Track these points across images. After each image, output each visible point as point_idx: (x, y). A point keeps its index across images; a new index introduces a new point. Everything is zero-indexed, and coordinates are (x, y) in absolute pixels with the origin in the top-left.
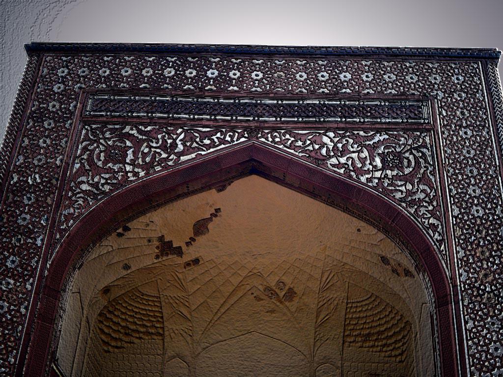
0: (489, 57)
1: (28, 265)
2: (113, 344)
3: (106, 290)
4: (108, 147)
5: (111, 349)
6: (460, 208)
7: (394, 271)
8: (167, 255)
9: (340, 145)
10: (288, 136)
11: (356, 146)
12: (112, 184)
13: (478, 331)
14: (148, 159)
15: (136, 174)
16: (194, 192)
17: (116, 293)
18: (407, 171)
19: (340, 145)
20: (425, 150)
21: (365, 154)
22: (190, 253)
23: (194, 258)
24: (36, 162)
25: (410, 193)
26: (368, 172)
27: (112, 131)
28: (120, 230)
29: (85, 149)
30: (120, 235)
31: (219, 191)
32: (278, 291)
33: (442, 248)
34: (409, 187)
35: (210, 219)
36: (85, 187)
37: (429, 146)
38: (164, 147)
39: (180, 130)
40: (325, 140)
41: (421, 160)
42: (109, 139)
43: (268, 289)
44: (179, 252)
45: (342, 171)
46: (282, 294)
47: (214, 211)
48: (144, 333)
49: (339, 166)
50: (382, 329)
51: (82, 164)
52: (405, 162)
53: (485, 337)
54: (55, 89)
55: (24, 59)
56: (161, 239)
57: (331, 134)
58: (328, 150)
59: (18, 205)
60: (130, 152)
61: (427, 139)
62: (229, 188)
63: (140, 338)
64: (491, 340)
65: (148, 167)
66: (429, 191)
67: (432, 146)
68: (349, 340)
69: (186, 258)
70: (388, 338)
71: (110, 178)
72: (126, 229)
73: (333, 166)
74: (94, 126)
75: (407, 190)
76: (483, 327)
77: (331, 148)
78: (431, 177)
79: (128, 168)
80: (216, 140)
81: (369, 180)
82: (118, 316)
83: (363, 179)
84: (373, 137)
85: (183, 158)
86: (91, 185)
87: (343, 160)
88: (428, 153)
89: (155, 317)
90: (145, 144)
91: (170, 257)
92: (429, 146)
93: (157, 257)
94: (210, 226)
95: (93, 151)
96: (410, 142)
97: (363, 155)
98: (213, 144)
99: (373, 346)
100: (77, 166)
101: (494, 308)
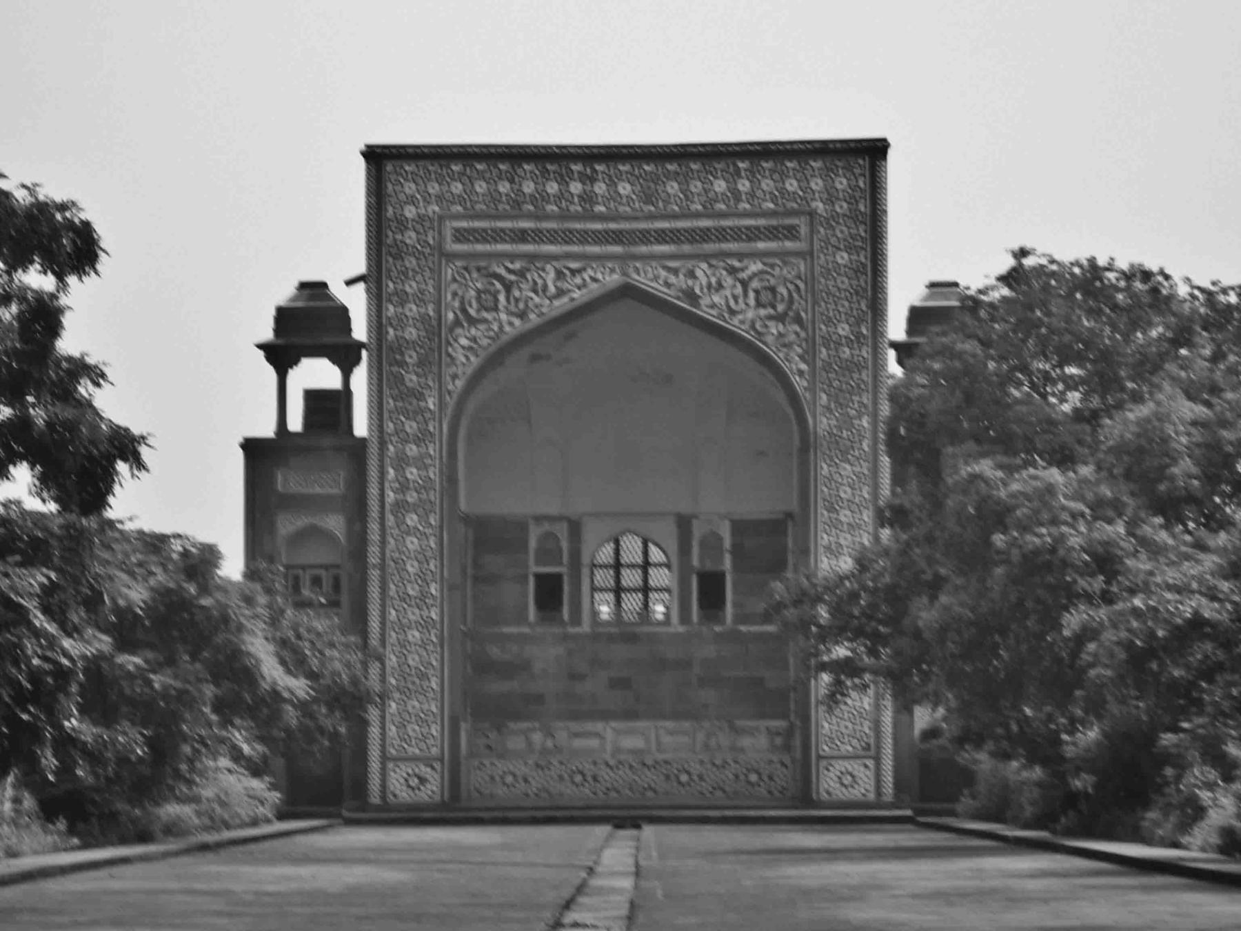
0: (876, 150)
4: (479, 292)
9: (713, 280)
12: (489, 338)
14: (521, 306)
15: (511, 324)
18: (781, 308)
19: (713, 280)
20: (798, 282)
27: (479, 269)
29: (455, 294)
34: (781, 327)
36: (464, 342)
38: (535, 291)
39: (548, 267)
44: (548, 357)
52: (779, 296)
54: (408, 215)
55: (361, 162)
58: (701, 289)
59: (402, 364)
60: (502, 298)
65: (522, 315)
66: (798, 329)
81: (742, 322)
83: (736, 321)
87: (716, 299)
88: (802, 286)
95: (463, 298)
100: (451, 316)
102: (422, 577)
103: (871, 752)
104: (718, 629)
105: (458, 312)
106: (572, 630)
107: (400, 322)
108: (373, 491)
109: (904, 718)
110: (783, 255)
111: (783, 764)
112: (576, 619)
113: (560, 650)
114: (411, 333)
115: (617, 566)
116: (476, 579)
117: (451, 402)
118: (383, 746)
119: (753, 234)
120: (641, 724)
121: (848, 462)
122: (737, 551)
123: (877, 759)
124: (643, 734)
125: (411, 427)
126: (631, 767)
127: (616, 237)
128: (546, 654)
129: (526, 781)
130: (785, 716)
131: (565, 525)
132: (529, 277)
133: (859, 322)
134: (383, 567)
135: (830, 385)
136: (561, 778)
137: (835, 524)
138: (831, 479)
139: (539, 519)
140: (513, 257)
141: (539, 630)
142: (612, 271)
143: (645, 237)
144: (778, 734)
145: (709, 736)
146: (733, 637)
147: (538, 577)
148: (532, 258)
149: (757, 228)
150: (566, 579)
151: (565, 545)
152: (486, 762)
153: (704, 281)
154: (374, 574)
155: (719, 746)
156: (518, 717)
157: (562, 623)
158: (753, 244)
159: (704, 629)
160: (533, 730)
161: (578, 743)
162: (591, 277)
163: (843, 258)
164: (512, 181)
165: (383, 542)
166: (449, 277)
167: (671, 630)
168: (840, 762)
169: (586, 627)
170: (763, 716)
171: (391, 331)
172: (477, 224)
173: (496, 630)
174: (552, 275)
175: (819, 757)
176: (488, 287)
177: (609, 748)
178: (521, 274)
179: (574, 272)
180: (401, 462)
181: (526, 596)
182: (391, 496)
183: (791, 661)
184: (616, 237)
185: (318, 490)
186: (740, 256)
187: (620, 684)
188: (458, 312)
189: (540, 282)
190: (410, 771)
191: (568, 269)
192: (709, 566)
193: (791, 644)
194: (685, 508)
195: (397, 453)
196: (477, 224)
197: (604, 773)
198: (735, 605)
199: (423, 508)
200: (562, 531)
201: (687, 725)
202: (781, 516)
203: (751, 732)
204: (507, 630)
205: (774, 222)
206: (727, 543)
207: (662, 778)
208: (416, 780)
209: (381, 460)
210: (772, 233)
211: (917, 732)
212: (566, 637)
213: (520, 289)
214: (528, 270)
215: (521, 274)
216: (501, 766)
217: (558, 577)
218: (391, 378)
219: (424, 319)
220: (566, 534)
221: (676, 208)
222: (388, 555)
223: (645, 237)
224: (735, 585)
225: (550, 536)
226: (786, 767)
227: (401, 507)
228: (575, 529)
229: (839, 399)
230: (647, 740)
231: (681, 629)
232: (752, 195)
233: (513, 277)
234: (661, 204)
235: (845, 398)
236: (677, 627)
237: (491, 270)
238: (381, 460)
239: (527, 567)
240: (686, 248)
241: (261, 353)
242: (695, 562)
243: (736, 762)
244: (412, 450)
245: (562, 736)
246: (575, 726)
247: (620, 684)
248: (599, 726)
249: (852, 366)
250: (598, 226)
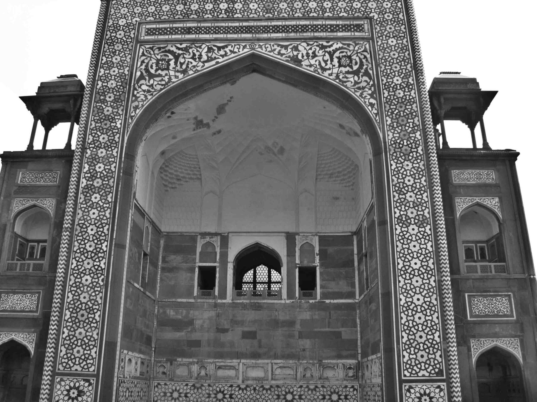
1: (113, 140)
2: (170, 186)
3: (163, 153)
4: (158, 61)
5: (168, 189)
6: (389, 92)
7: (348, 133)
8: (200, 128)
9: (310, 52)
10: (276, 47)
11: (321, 52)
13: (399, 170)
14: (184, 67)
16: (215, 87)
17: (168, 155)
19: (310, 52)
21: (327, 57)
22: (215, 126)
23: (218, 128)
24: (112, 73)
25: (356, 83)
26: (329, 69)
27: (159, 49)
28: (168, 115)
29: (143, 62)
30: (169, 117)
31: (232, 84)
32: (273, 149)
33: (377, 118)
35: (227, 104)
37: (368, 51)
38: (193, 58)
39: (204, 46)
40: (300, 48)
41: (364, 61)
42: (158, 54)
43: (267, 148)
45: (312, 69)
46: (276, 151)
47: (229, 99)
48: (189, 178)
49: (311, 66)
50: (341, 170)
51: (142, 73)
53: (403, 174)
56: (196, 118)
57: (304, 44)
58: (303, 57)
59: (104, 101)
60: (172, 63)
61: (367, 46)
62: (238, 82)
63: (187, 182)
64: (406, 175)
67: (370, 52)
68: (319, 177)
69: (212, 130)
70: (344, 175)
71: (160, 81)
72: (173, 113)
73: (307, 66)
74: (147, 46)
75: (355, 81)
76: (402, 167)
77: (305, 54)
78: (371, 72)
79: (172, 73)
80: (228, 51)
82: (172, 169)
84: (332, 46)
85: (207, 65)
86: (149, 86)
87: (313, 62)
89: (195, 168)
90: (182, 56)
91: (202, 129)
92: (368, 51)
93: (194, 130)
94: (227, 108)
95: (148, 63)
96: (356, 48)
97: (325, 58)
98: (226, 55)
99: (335, 181)
100: (138, 74)
101: (409, 156)
102: (98, 239)
103: (442, 376)
104: (311, 301)
105: (144, 72)
106: (219, 301)
107: (107, 78)
108: (73, 179)
109: (465, 349)
110: (354, 39)
111: (355, 389)
112: (223, 295)
113: (212, 313)
114: (112, 84)
115: (255, 282)
116: (163, 269)
117: (132, 123)
118: (54, 362)
119: (334, 29)
120: (260, 361)
121: (409, 160)
122: (323, 254)
123: (449, 381)
124: (262, 367)
125: (103, 138)
126: (255, 389)
127: (248, 29)
128: (204, 317)
129: (186, 396)
130: (354, 357)
131: (219, 237)
132: (190, 51)
133: (407, 76)
134: (72, 230)
135: (392, 113)
136: (209, 396)
137: (403, 202)
138: (398, 172)
139: (204, 235)
140: (181, 41)
141: (199, 300)
142: (244, 47)
143: (266, 29)
144: (350, 368)
145: (305, 370)
146: (321, 306)
147: (200, 268)
148: (194, 41)
149: (338, 26)
150: (218, 269)
151: (218, 250)
152: (162, 383)
153: (305, 52)
154: (65, 235)
155: (312, 376)
156: (184, 355)
157: (215, 298)
158: (335, 34)
159: (303, 301)
160: (192, 363)
161: (221, 373)
162: (230, 51)
163: (392, 42)
164: (185, 4)
165: (75, 213)
166: (140, 54)
167: (283, 302)
168: (420, 385)
169: (229, 299)
170: (340, 357)
171: (100, 83)
172: (161, 26)
173: (174, 300)
174: (206, 50)
175: (401, 382)
176: (164, 57)
177: (241, 378)
178: (186, 50)
179: (219, 48)
180: (94, 160)
181: (194, 280)
182: (84, 182)
183: (358, 320)
184: (248, 29)
185: (42, 183)
186: (328, 39)
187: (249, 335)
188: (144, 72)
189: (197, 54)
190: (72, 384)
191: (214, 46)
192: (306, 263)
193: (358, 311)
194: (292, 230)
195: (91, 155)
196: (161, 26)
197: (237, 393)
198: (321, 287)
199: (103, 190)
200: (217, 242)
201: (291, 362)
202: (350, 234)
203: (333, 368)
204: (179, 300)
205: (348, 23)
206: (317, 250)
207: (275, 397)
208: (76, 392)
209: (81, 160)
210: (346, 28)
211: (474, 360)
212: (216, 305)
213: (184, 58)
214: (192, 48)
215: (186, 50)
216: (171, 386)
217: (215, 268)
218: (96, 109)
219: (121, 75)
220: (219, 244)
221: (285, 15)
222: (76, 223)
223: (266, 29)
224: (320, 273)
225: (209, 244)
226: (355, 389)
227: (89, 188)
228: (225, 241)
229: (399, 121)
230: (266, 372)
231: (288, 302)
232: (332, 9)
233: (181, 52)
234: (276, 13)
235: (403, 121)
236: (285, 300)
237: (167, 49)
238: (81, 160)
239: (195, 263)
240: (292, 35)
241: (23, 105)
242: (298, 261)
243: (323, 387)
244: (102, 153)
245: (211, 368)
246: (220, 362)
247: (249, 335)
248: (235, 362)
249: (405, 102)
250: (237, 24)
